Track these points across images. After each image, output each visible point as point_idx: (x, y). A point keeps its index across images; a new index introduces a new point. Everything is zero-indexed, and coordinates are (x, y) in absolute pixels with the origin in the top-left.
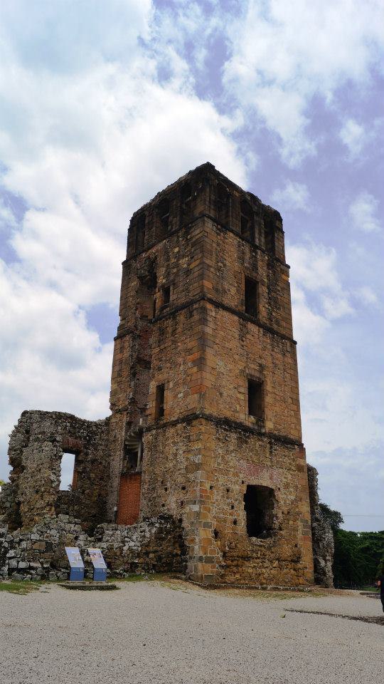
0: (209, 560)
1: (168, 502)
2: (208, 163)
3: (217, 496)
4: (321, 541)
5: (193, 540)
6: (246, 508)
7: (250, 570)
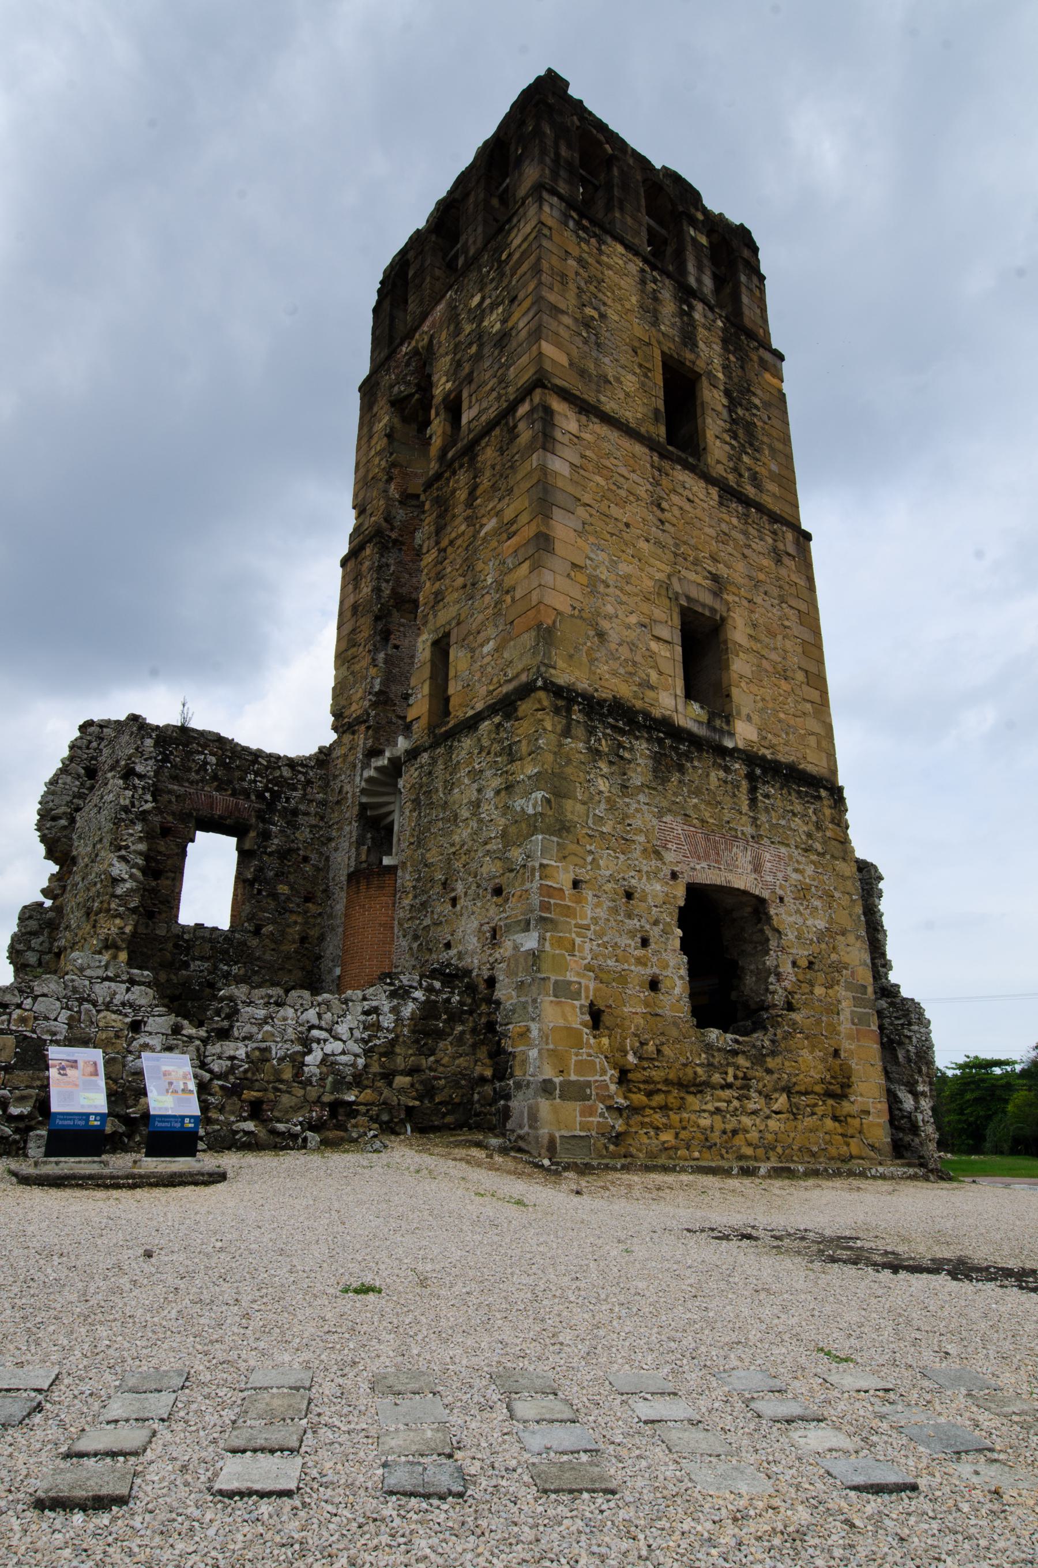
1: (459, 934)
2: (550, 71)
4: (901, 1043)
5: (525, 1034)
6: (686, 946)
7: (705, 1122)
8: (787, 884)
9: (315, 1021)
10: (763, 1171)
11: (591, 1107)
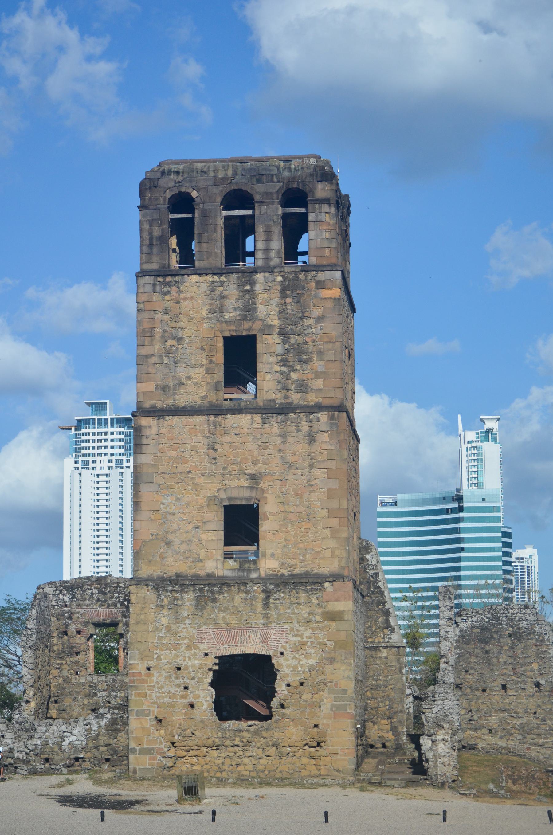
0: (148, 752)
3: (155, 677)
7: (219, 761)
8: (287, 645)
9: (66, 730)
10: (231, 780)
11: (154, 757)
